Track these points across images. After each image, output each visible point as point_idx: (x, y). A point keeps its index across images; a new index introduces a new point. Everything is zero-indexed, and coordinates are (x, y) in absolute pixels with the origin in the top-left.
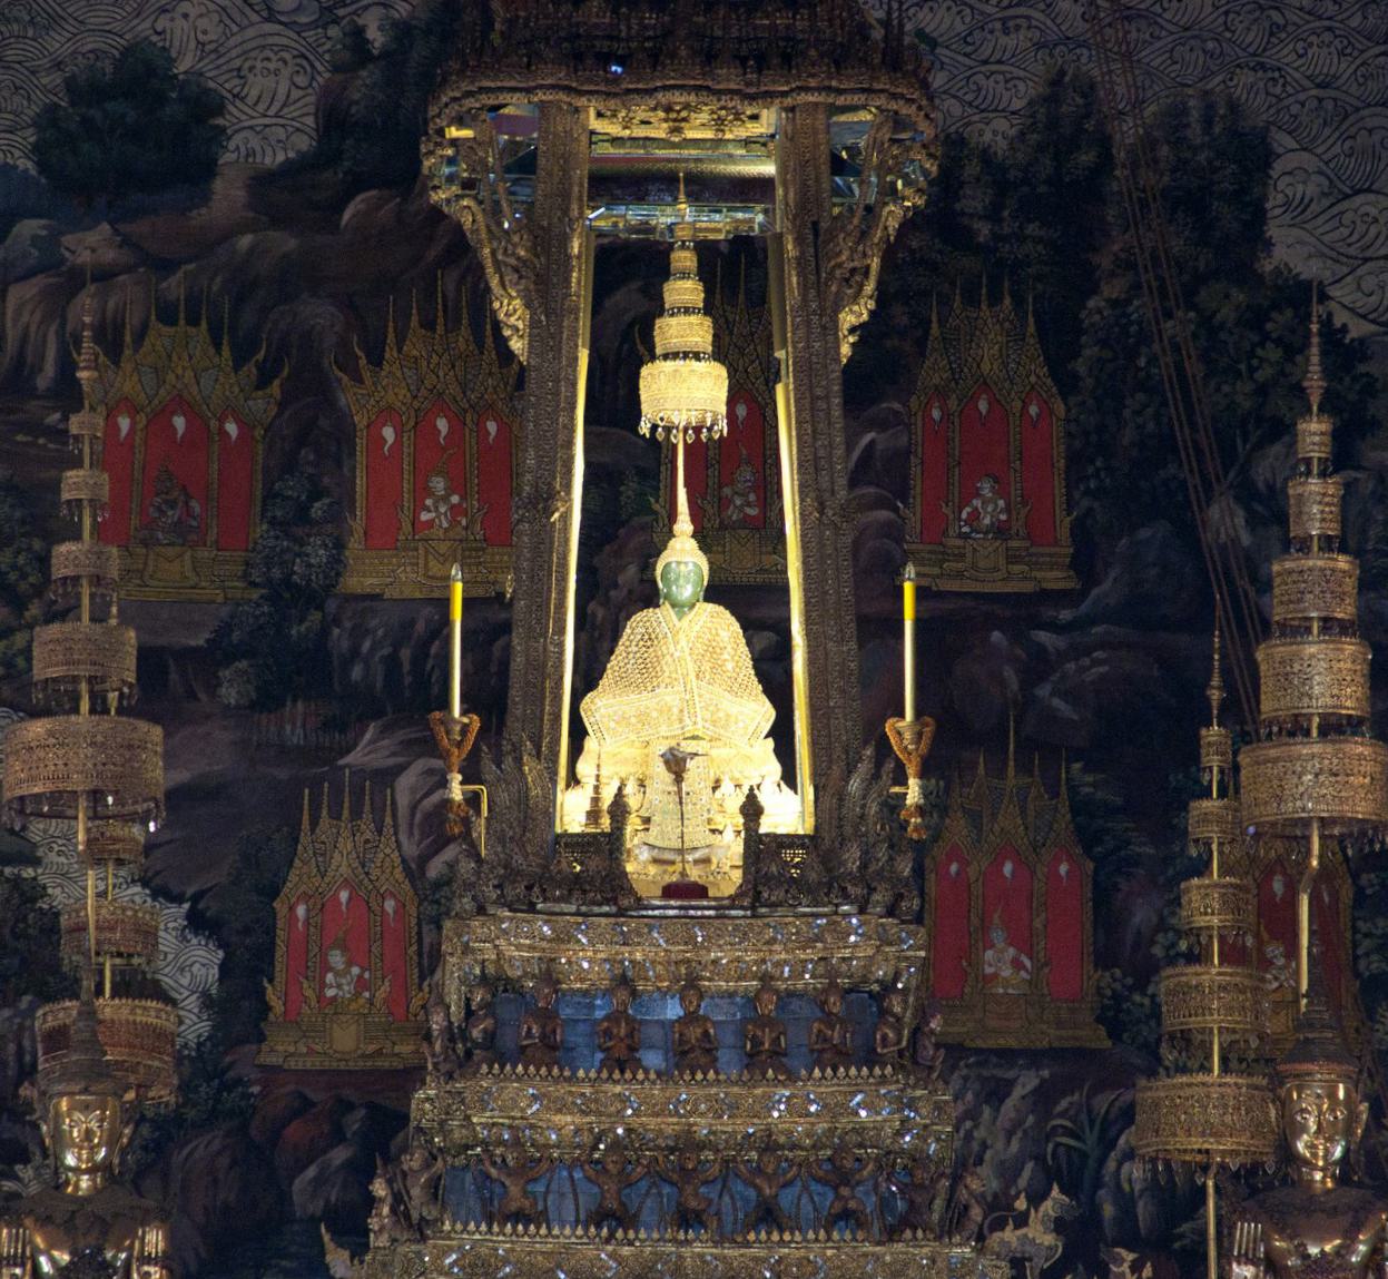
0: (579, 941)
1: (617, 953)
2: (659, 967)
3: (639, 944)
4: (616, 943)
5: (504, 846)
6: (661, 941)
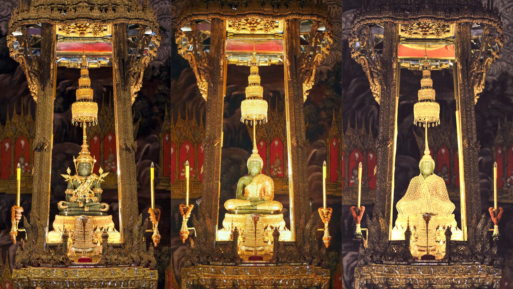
0: (396, 272)
1: (407, 276)
2: (420, 281)
3: (414, 273)
4: (407, 273)
5: (373, 245)
6: (421, 272)
